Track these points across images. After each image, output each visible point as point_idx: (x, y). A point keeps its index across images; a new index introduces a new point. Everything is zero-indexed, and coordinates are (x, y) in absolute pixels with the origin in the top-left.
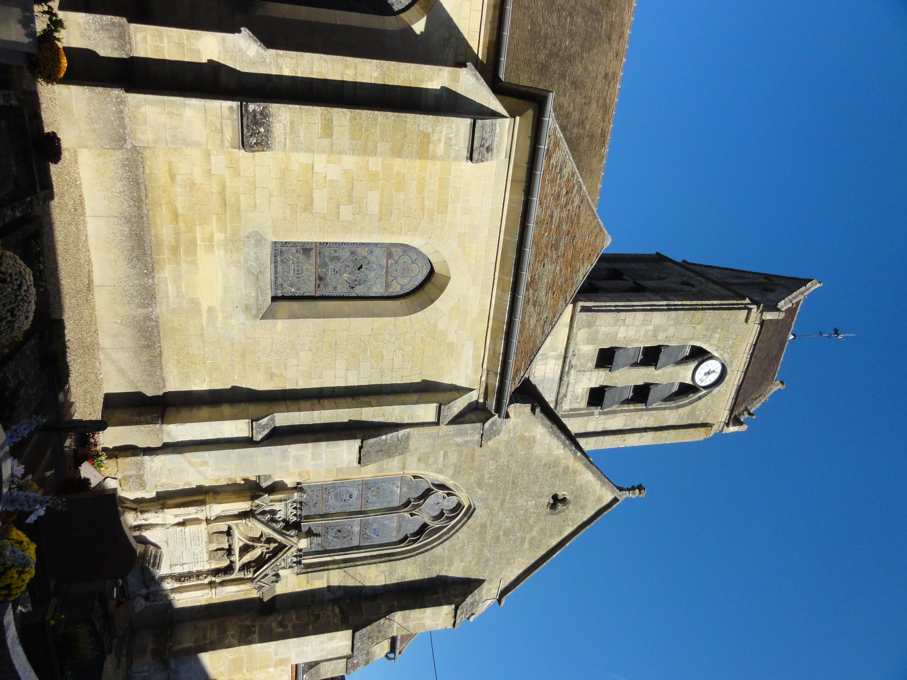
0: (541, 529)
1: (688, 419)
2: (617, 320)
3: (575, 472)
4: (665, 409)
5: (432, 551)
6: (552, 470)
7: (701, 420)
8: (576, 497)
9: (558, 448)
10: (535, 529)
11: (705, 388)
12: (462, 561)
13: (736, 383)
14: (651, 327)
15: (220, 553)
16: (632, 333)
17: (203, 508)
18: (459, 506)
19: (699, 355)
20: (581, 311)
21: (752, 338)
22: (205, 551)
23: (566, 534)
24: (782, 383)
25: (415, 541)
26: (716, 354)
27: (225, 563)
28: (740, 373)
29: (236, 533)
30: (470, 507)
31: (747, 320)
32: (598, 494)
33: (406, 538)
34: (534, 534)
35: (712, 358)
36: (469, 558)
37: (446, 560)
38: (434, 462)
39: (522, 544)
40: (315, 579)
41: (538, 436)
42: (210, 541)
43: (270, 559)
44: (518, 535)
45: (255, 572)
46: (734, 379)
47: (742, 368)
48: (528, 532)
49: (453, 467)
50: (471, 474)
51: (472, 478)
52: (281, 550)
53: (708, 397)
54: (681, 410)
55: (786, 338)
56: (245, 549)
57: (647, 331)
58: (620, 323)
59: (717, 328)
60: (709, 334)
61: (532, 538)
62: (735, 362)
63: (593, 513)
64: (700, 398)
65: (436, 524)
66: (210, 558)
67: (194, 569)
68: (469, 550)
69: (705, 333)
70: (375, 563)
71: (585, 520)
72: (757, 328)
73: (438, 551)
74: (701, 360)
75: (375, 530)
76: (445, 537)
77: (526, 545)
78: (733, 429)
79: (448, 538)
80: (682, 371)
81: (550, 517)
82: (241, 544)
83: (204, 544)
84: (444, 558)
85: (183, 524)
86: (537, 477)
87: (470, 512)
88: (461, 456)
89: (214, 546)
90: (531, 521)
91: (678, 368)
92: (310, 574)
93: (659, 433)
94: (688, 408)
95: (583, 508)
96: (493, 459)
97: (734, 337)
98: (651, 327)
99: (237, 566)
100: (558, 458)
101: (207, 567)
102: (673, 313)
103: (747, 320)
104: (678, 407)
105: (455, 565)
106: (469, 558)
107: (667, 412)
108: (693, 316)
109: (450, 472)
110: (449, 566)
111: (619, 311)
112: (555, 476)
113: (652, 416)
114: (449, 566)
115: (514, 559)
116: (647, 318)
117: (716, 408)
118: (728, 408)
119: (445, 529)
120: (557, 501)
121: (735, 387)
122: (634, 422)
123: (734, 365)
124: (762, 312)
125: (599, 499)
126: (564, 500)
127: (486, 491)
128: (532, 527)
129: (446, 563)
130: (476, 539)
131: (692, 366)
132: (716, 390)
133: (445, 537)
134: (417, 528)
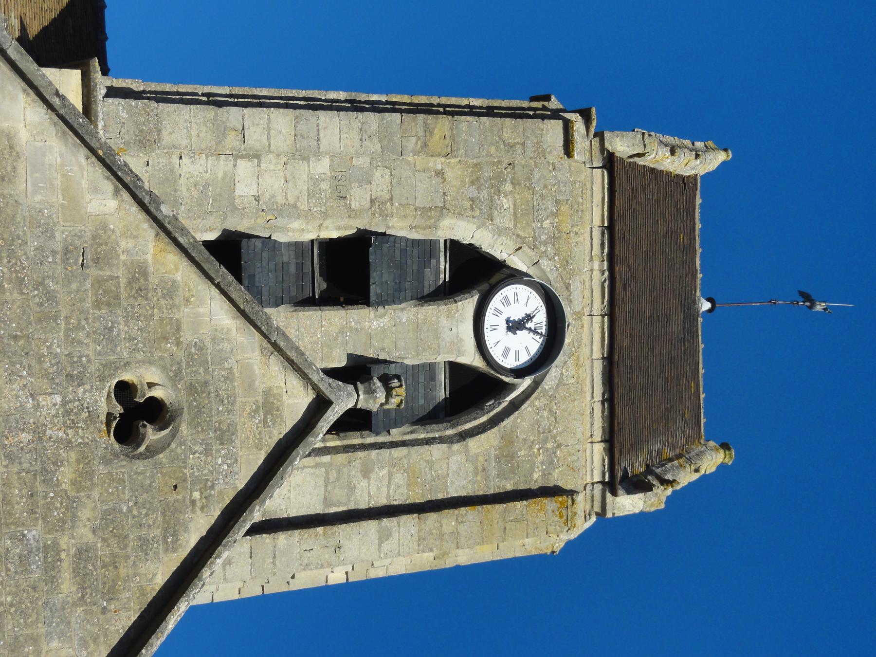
0: (105, 515)
1: (501, 475)
2: (222, 131)
3: (170, 290)
4: (428, 442)
6: (93, 272)
7: (537, 479)
8: (191, 389)
9: (95, 189)
10: (85, 514)
11: (520, 373)
13: (597, 353)
14: (322, 167)
16: (272, 183)
19: (475, 273)
20: (107, 96)
21: (596, 214)
23: (191, 540)
24: (725, 446)
26: (518, 263)
28: (597, 320)
31: (568, 151)
32: (260, 386)
34: (84, 533)
35: (515, 276)
39: (51, 567)
41: (23, 136)
44: (32, 534)
46: (586, 337)
47: (598, 306)
48: (61, 526)
53: (536, 401)
54: (473, 444)
55: (691, 313)
57: (315, 181)
58: (232, 141)
59: (499, 179)
60: (484, 195)
61: (83, 554)
62: (576, 285)
63: (259, 458)
64: (515, 406)
69: (472, 192)
71: (241, 484)
72: (600, 178)
74: (485, 286)
77: (67, 586)
78: (628, 504)
80: (444, 322)
81: (124, 468)
86: (51, 296)
90: (66, 475)
91: (430, 310)
93: (432, 517)
94: (492, 437)
95: (225, 436)
97: (552, 208)
98: (322, 167)
100: (105, 227)
102: (372, 119)
103: (568, 151)
104: (463, 436)
107: (438, 450)
108: (428, 131)
111: (220, 104)
112: (108, 299)
113: (396, 464)
115: (34, 640)
116: (302, 127)
117: (565, 424)
118: (598, 435)
120: (136, 416)
121: (598, 367)
122: (352, 488)
123: (576, 296)
124: (599, 135)
125: (269, 406)
126: (156, 412)
128: (72, 506)
131: (468, 305)
132: (554, 373)
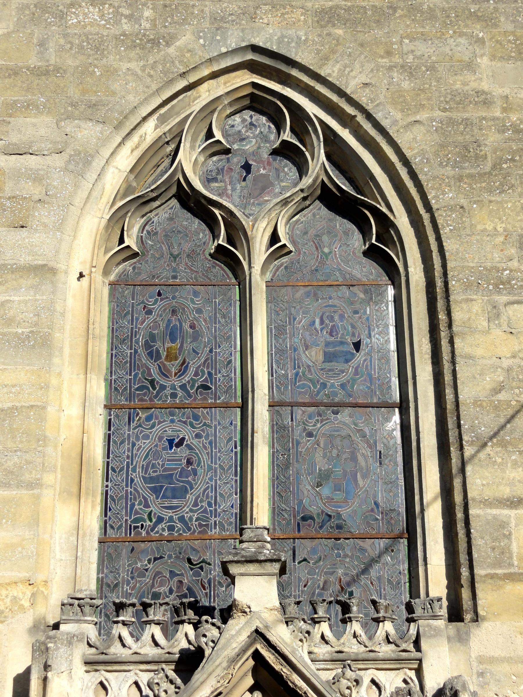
5: (416, 162)
12: (470, 66)
18: (257, 102)
25: (386, 223)
30: (252, 67)
33: (373, 253)
36: (461, 47)
37: (455, 115)
38: (37, 178)
40: (506, 551)
49: (69, 127)
50: (110, 72)
51: (125, 66)
52: (277, 676)
65: (318, 161)
68: (421, 48)
70: (451, 342)
73: (415, 142)
75: (329, 357)
76: (367, 126)
79: (369, 117)
84: (451, 122)
87: (268, 61)
88: (28, 106)
92: (479, 571)
96: (62, 16)
105: (485, 86)
106: (461, 47)
109: (87, 132)
110: (487, 103)
114: (487, 103)
119: (345, 134)
127: (185, 22)
129: (474, 113)
130: (379, 33)
133: (367, 126)
134: (342, 224)
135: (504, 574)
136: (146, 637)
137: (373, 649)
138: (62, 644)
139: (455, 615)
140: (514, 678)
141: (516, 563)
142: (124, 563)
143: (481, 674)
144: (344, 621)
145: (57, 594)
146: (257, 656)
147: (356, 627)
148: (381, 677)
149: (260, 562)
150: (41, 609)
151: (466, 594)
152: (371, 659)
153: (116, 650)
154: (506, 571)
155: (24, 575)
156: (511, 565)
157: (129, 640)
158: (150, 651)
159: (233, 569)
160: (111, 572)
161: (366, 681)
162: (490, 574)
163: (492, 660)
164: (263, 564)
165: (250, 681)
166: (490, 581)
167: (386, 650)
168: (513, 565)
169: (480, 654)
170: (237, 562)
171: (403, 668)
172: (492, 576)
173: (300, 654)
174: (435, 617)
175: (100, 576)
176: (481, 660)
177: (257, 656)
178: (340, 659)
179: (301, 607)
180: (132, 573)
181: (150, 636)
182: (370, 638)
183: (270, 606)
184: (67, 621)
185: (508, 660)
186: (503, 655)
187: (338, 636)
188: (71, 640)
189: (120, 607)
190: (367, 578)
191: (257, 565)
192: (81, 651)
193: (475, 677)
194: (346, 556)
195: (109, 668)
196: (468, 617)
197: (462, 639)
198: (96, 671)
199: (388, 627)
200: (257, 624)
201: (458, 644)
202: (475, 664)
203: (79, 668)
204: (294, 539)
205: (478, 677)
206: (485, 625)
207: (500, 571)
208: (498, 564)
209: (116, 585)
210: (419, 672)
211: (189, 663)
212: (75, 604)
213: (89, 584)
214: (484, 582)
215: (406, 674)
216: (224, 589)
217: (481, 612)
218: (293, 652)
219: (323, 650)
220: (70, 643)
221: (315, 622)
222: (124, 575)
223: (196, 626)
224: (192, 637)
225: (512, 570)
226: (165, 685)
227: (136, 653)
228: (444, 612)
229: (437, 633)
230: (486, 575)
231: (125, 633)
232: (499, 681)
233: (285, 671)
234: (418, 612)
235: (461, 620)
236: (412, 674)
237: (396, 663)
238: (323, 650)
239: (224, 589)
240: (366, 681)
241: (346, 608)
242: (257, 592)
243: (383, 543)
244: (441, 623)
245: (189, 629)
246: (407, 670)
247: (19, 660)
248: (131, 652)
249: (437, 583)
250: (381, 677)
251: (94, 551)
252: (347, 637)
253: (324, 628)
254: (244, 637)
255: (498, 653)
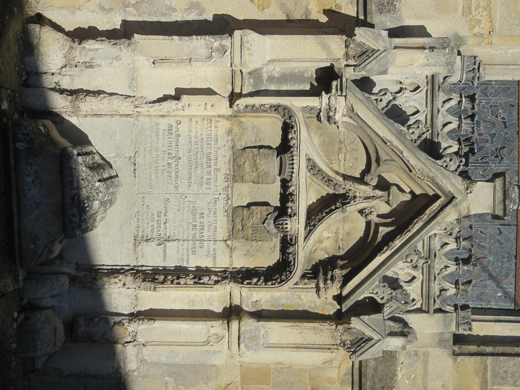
15: (259, 212)
17: (226, 41)
22: (221, 204)
27: (268, 256)
29: (308, 144)
40: (504, 381)
42: (236, 176)
43: (389, 238)
45: (347, 279)
52: (421, 211)
56: (324, 207)
66: (233, 233)
67: (192, 264)
82: (313, 198)
83: (221, 184)
85: (178, 95)
89: (244, 193)
92: (489, 360)
99: (301, 265)
101: (223, 261)
135: (487, 378)
136: (450, 118)
137: (437, 279)
138: (447, 58)
139: (458, 339)
140: (413, 376)
141: (495, 387)
142: (503, 100)
143: (416, 354)
144: (456, 260)
145: (482, 52)
146: (436, 197)
147: (453, 268)
148: (417, 284)
149: (504, 201)
150: (471, 41)
151: (473, 348)
152: (430, 277)
153: (441, 97)
154: (489, 379)
155: (497, 27)
156: (493, 384)
157: (448, 105)
158: (440, 121)
159: (499, 182)
160: (496, 91)
161: (414, 273)
162: (487, 367)
163: (426, 363)
164: (502, 203)
165: (418, 192)
166: (482, 367)
167: (436, 288)
168: (493, 385)
169: (430, 355)
170: (504, 184)
171: (423, 299)
172: (485, 369)
173: (436, 229)
174: (458, 325)
175: (493, 83)
176: (426, 355)
177: (436, 197)
178: (431, 255)
179: (469, 230)
180: (495, 106)
181: (451, 121)
182: (444, 278)
183: (471, 207)
184: (463, 60)
185: (425, 374)
186: (429, 370)
187: (446, 255)
188: (450, 64)
189: (472, 98)
190: (485, 277)
191: (502, 199)
192: (441, 71)
193: (415, 349)
194: (503, 263)
195: (429, 92)
196: (456, 348)
197: (441, 343)
198: (427, 83)
199: (452, 291)
200: (459, 198)
201: (437, 340)
202: (423, 350)
203: (429, 72)
204: (517, 225)
205: (414, 351)
206: (450, 361)
207: (489, 375)
208: (495, 374)
209: (486, 95)
210: (420, 311)
211: (431, 148)
212: (475, 65)
213: (490, 75)
214: (481, 363)
215: (419, 301)
216: (481, 173)
217: (460, 358)
218: (438, 223)
219: (436, 244)
220: (448, 64)
221: (457, 239)
222: (493, 100)
223: (456, 153)
224: (449, 151)
225: (489, 384)
226: (417, 132)
227: (439, 111)
228: (461, 332)
229: (447, 326)
230: (486, 365)
231: (453, 103)
232: (411, 366)
233: (425, 217)
234: (462, 314)
235: (454, 344)
236: (418, 306)
237: (427, 296)
238: (436, 244)
239: (481, 173)
240: (414, 273)
241: (466, 261)
242: (481, 198)
243: (511, 290)
244: (453, 329)
245: (455, 148)
246: (421, 302)
247: (436, 28)
248: (440, 107)
249: (482, 328)
250: (417, 284)
251: (512, 77)
252: (446, 261)
253: (453, 246)
254: (450, 188)
255: (431, 368)
